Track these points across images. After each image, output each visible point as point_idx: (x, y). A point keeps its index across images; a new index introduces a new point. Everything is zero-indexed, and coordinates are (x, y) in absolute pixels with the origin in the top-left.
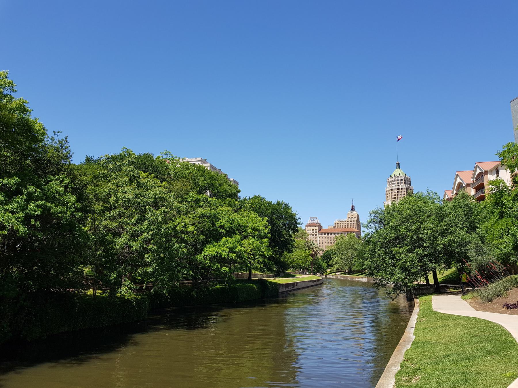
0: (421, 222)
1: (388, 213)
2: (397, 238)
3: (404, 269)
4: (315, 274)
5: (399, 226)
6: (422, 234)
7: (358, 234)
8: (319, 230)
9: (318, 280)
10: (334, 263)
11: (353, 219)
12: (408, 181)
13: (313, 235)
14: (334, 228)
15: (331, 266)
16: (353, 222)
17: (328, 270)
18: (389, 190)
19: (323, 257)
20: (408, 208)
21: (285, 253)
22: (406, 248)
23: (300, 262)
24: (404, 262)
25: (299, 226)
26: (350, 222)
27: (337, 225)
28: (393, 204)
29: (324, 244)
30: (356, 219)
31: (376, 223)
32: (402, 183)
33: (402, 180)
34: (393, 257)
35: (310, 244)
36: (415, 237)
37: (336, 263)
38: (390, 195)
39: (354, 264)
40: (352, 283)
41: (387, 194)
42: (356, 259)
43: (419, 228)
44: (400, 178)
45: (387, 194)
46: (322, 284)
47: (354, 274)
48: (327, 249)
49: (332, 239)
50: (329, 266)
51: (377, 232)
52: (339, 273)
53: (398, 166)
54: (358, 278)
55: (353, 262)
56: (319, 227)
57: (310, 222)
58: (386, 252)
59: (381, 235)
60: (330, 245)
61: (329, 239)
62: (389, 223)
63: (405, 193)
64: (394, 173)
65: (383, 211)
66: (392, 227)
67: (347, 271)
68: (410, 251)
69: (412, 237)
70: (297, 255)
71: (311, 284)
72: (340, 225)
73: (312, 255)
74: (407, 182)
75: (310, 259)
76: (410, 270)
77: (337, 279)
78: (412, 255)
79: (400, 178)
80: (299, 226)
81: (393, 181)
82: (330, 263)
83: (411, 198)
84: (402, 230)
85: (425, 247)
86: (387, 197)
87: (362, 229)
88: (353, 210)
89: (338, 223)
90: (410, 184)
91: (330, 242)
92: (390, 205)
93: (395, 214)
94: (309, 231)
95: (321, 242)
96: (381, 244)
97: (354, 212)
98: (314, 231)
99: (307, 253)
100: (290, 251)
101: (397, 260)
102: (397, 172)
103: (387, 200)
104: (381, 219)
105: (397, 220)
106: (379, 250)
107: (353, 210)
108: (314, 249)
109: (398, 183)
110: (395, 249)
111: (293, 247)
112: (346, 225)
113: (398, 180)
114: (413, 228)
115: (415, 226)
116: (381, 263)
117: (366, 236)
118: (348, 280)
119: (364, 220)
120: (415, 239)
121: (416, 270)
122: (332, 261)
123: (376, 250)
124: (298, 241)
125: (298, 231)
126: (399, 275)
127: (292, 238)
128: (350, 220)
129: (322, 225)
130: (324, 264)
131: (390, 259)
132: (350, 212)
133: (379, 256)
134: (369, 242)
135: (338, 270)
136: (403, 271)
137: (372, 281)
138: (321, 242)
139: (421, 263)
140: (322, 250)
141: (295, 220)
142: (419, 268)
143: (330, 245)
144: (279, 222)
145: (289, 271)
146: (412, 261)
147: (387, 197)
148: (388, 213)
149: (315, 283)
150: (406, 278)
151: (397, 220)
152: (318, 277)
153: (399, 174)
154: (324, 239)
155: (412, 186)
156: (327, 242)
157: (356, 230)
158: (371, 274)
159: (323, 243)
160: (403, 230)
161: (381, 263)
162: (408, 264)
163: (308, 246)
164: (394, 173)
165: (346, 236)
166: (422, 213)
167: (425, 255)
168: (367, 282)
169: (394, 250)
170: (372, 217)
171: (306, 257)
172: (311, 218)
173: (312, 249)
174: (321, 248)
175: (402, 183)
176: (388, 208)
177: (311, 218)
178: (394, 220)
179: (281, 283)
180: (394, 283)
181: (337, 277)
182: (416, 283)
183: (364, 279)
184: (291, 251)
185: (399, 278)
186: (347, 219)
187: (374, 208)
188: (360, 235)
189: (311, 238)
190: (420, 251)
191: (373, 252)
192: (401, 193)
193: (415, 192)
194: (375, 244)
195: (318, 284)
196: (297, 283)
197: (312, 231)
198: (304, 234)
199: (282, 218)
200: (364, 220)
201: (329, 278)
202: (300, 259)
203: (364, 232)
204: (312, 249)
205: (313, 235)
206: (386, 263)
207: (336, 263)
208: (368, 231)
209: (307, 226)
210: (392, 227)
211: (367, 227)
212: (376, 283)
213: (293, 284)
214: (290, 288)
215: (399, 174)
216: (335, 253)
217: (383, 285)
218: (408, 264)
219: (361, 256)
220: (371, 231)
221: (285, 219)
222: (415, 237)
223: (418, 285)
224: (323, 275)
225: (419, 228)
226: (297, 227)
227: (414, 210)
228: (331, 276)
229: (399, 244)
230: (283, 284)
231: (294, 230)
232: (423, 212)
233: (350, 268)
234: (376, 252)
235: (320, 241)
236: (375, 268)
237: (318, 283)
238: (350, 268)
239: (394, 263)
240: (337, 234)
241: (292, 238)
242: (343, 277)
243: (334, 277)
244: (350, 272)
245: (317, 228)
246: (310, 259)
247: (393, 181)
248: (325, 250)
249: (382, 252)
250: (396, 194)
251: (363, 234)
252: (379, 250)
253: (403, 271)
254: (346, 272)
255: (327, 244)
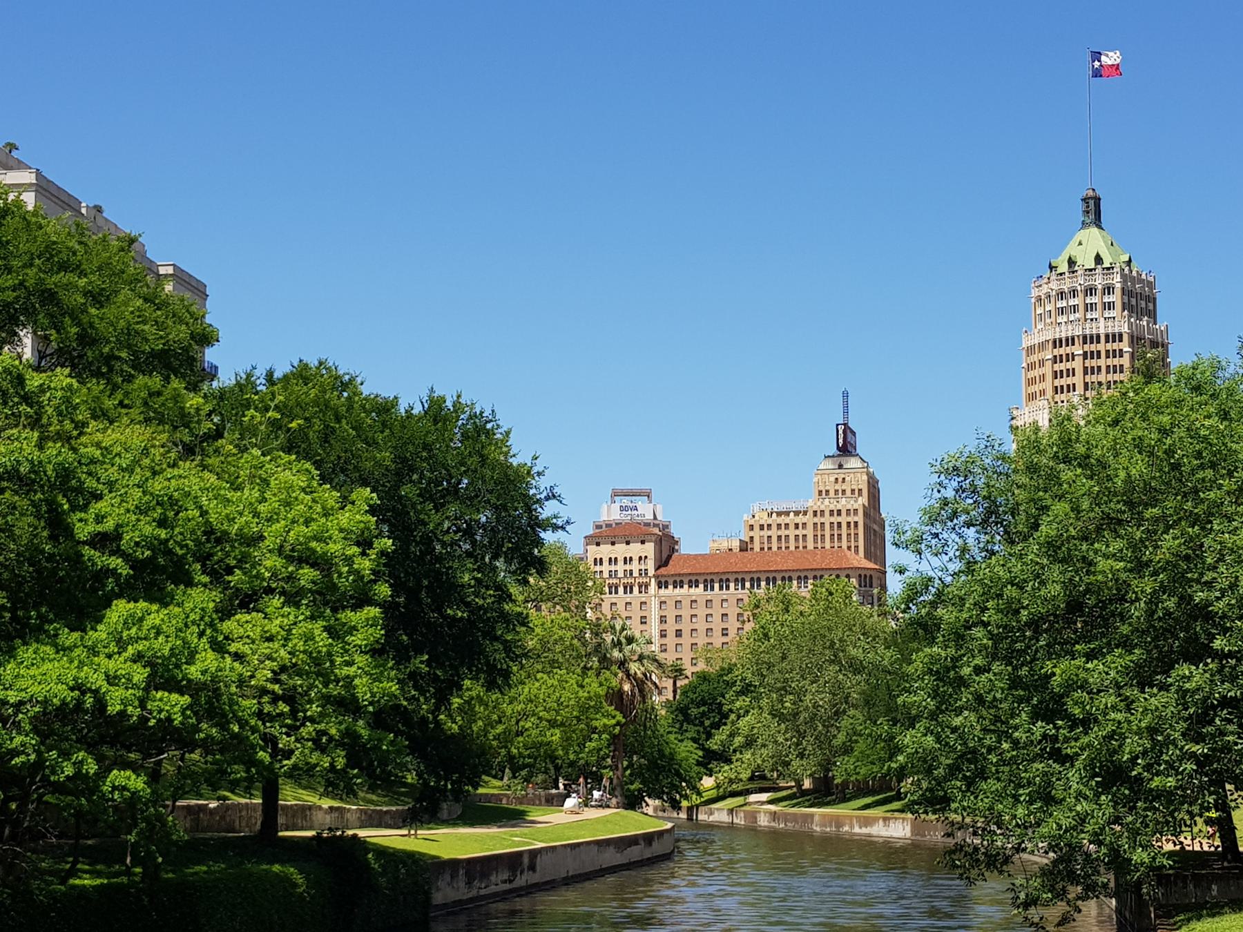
0: (1203, 522)
1: (1032, 469)
2: (1075, 606)
3: (1112, 775)
4: (632, 802)
5: (1085, 538)
6: (1209, 585)
7: (872, 582)
8: (663, 562)
9: (649, 838)
10: (738, 740)
11: (843, 504)
12: (1140, 296)
13: (628, 588)
14: (744, 547)
15: (723, 757)
16: (843, 519)
17: (708, 782)
18: (1042, 346)
19: (681, 712)
20: (1139, 444)
21: (472, 687)
22: (1118, 660)
23: (555, 736)
24: (1110, 737)
25: (548, 536)
26: (827, 519)
27: (756, 533)
28: (1061, 421)
29: (686, 640)
30: (863, 500)
31: (969, 525)
32: (1110, 306)
33: (1109, 289)
34: (1051, 710)
35: (608, 638)
36: (1171, 604)
37: (750, 743)
38: (1048, 369)
39: (847, 750)
40: (835, 847)
41: (1031, 367)
42: (854, 718)
43: (1193, 554)
44: (1099, 282)
45: (1031, 367)
46: (667, 857)
47: (845, 799)
48: (701, 666)
49: (733, 611)
50: (712, 759)
51: (970, 568)
52: (764, 797)
53: (1094, 211)
54: (867, 822)
55: (841, 738)
56: (659, 542)
57: (612, 513)
58: (1015, 683)
59: (992, 591)
60: (718, 640)
61: (717, 612)
62: (1036, 526)
63: (1126, 361)
64: (1072, 250)
65: (1004, 458)
66: (1052, 547)
67: (807, 784)
68: (1143, 678)
69: (1154, 600)
70: (541, 698)
71: (611, 857)
72: (774, 533)
73: (616, 698)
74: (1140, 300)
75: (609, 719)
76: (1139, 779)
77: (752, 830)
78: (1156, 700)
79: (1099, 282)
80: (548, 536)
81: (1061, 295)
82: (714, 744)
83: (1154, 389)
84: (1103, 564)
85: (1221, 656)
86: (1031, 382)
87: (894, 556)
88: (846, 449)
89: (763, 518)
90: (1152, 315)
91: (717, 624)
92: (1044, 421)
93: (1067, 474)
94: (606, 568)
95: (671, 627)
96: (992, 636)
97: (853, 463)
98: (635, 567)
99: (594, 686)
100: (497, 679)
101: (1074, 723)
102: (1089, 244)
103: (1032, 397)
104: (997, 499)
105: (1076, 509)
106: (978, 670)
107: (846, 449)
108: (634, 667)
109: (1089, 307)
110: (1065, 664)
111: (514, 652)
112: (809, 532)
113: (1090, 291)
114: (1162, 555)
115: (1170, 542)
116: (990, 740)
117: (912, 594)
118: (810, 836)
119: (904, 507)
120: (1168, 613)
121: (1171, 782)
122: (726, 729)
123: (966, 671)
124: (545, 620)
125: (541, 567)
126: (1081, 806)
127: (507, 607)
128: (827, 504)
129: (675, 532)
130: (686, 751)
131: (1035, 716)
132: (829, 465)
133: (980, 699)
134: (925, 629)
135: (759, 781)
136: (1105, 787)
137: (936, 837)
138: (671, 627)
139: (1198, 739)
140: (678, 672)
141: (529, 504)
142: (1190, 766)
143: (718, 640)
144: (436, 518)
145: (491, 787)
146: (1152, 731)
147: (1031, 382)
148: (1032, 469)
149: (635, 853)
150: (1117, 820)
151: (1076, 509)
152: (650, 818)
153: (1099, 260)
154: (686, 612)
155: (1161, 326)
156: (701, 626)
157: (860, 560)
158: (936, 801)
159: (677, 634)
160: (1109, 561)
161: (990, 740)
162: (1133, 745)
163: (600, 651)
164: (1072, 250)
165: (805, 592)
166: (1209, 473)
167: (1225, 702)
168: (915, 845)
169: (1060, 670)
170: (949, 493)
171: (584, 709)
172: (616, 494)
173: (622, 664)
174: (669, 658)
175: (1110, 306)
176: (1031, 443)
177: (616, 494)
178: (1060, 508)
179: (446, 855)
180: (1051, 848)
181: (753, 816)
182: (1169, 847)
183: (896, 829)
184: (506, 674)
185: (1082, 819)
186: (812, 503)
187: (960, 441)
188: (884, 588)
189: (612, 606)
190: (1193, 675)
191: (947, 679)
192: (1102, 362)
193: (1179, 358)
194: (959, 636)
195: (645, 858)
196: (534, 854)
197: (620, 568)
198: (576, 585)
199: (454, 491)
200: (904, 507)
201: (711, 826)
202: (553, 724)
203: (903, 568)
204: (622, 664)
205: (628, 588)
206: (1016, 744)
207: (750, 743)
208: (925, 568)
209: (594, 540)
210: (1052, 547)
211: (916, 545)
212: (959, 848)
213: (512, 862)
214: (498, 882)
215: (1099, 260)
216: (746, 690)
217: (997, 862)
218: (1133, 745)
219: (883, 701)
220: (935, 566)
221: (472, 500)
222: (1171, 604)
223: (1182, 856)
224: (676, 806)
225: (1193, 554)
226: (539, 543)
227: (1170, 452)
228: (719, 814)
229: (1084, 638)
230: (454, 864)
231: (523, 557)
232: (1213, 466)
233: (827, 766)
234: (961, 682)
235: (663, 620)
236: (953, 770)
237: (648, 854)
238: (827, 766)
239: (1055, 739)
240: (755, 582)
241: (507, 607)
242: (786, 818)
243: (739, 820)
244: (825, 792)
245: (649, 549)
246: (609, 719)
247: (1061, 295)
248: (689, 670)
249: (994, 681)
250: (1077, 364)
251: (895, 586)
252: (978, 670)
253: (1105, 787)
254: (804, 793)
255: (701, 640)
